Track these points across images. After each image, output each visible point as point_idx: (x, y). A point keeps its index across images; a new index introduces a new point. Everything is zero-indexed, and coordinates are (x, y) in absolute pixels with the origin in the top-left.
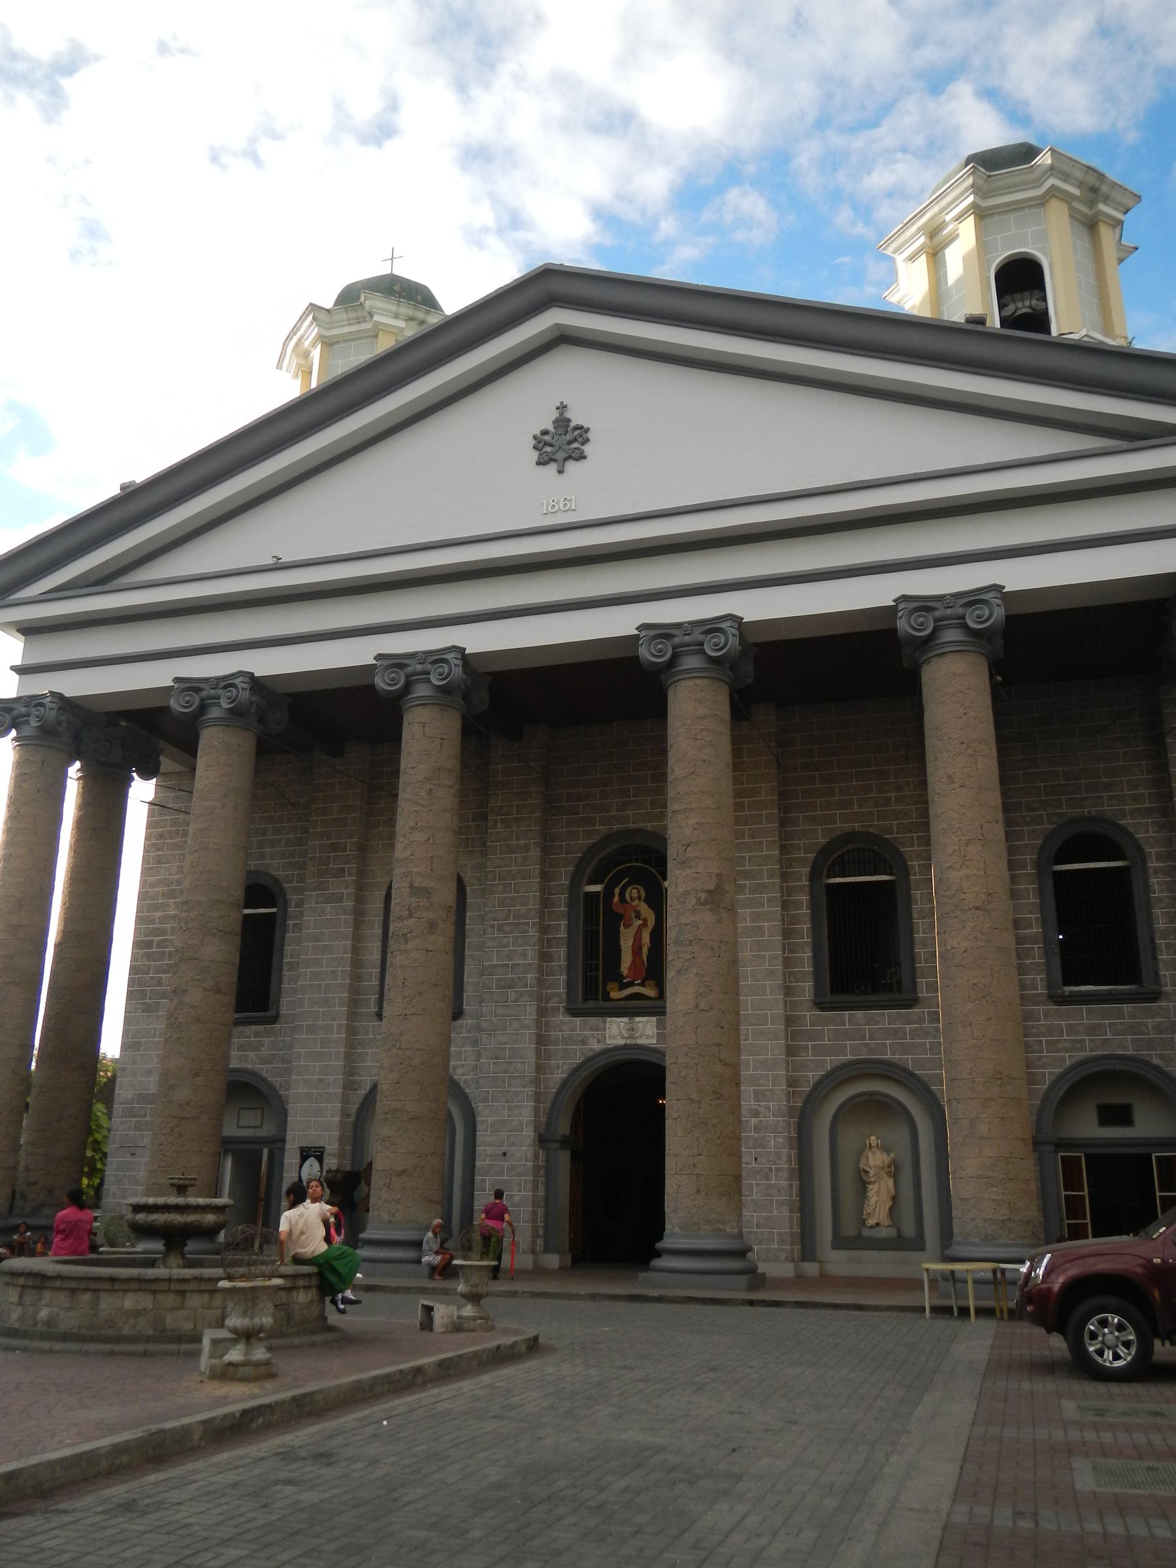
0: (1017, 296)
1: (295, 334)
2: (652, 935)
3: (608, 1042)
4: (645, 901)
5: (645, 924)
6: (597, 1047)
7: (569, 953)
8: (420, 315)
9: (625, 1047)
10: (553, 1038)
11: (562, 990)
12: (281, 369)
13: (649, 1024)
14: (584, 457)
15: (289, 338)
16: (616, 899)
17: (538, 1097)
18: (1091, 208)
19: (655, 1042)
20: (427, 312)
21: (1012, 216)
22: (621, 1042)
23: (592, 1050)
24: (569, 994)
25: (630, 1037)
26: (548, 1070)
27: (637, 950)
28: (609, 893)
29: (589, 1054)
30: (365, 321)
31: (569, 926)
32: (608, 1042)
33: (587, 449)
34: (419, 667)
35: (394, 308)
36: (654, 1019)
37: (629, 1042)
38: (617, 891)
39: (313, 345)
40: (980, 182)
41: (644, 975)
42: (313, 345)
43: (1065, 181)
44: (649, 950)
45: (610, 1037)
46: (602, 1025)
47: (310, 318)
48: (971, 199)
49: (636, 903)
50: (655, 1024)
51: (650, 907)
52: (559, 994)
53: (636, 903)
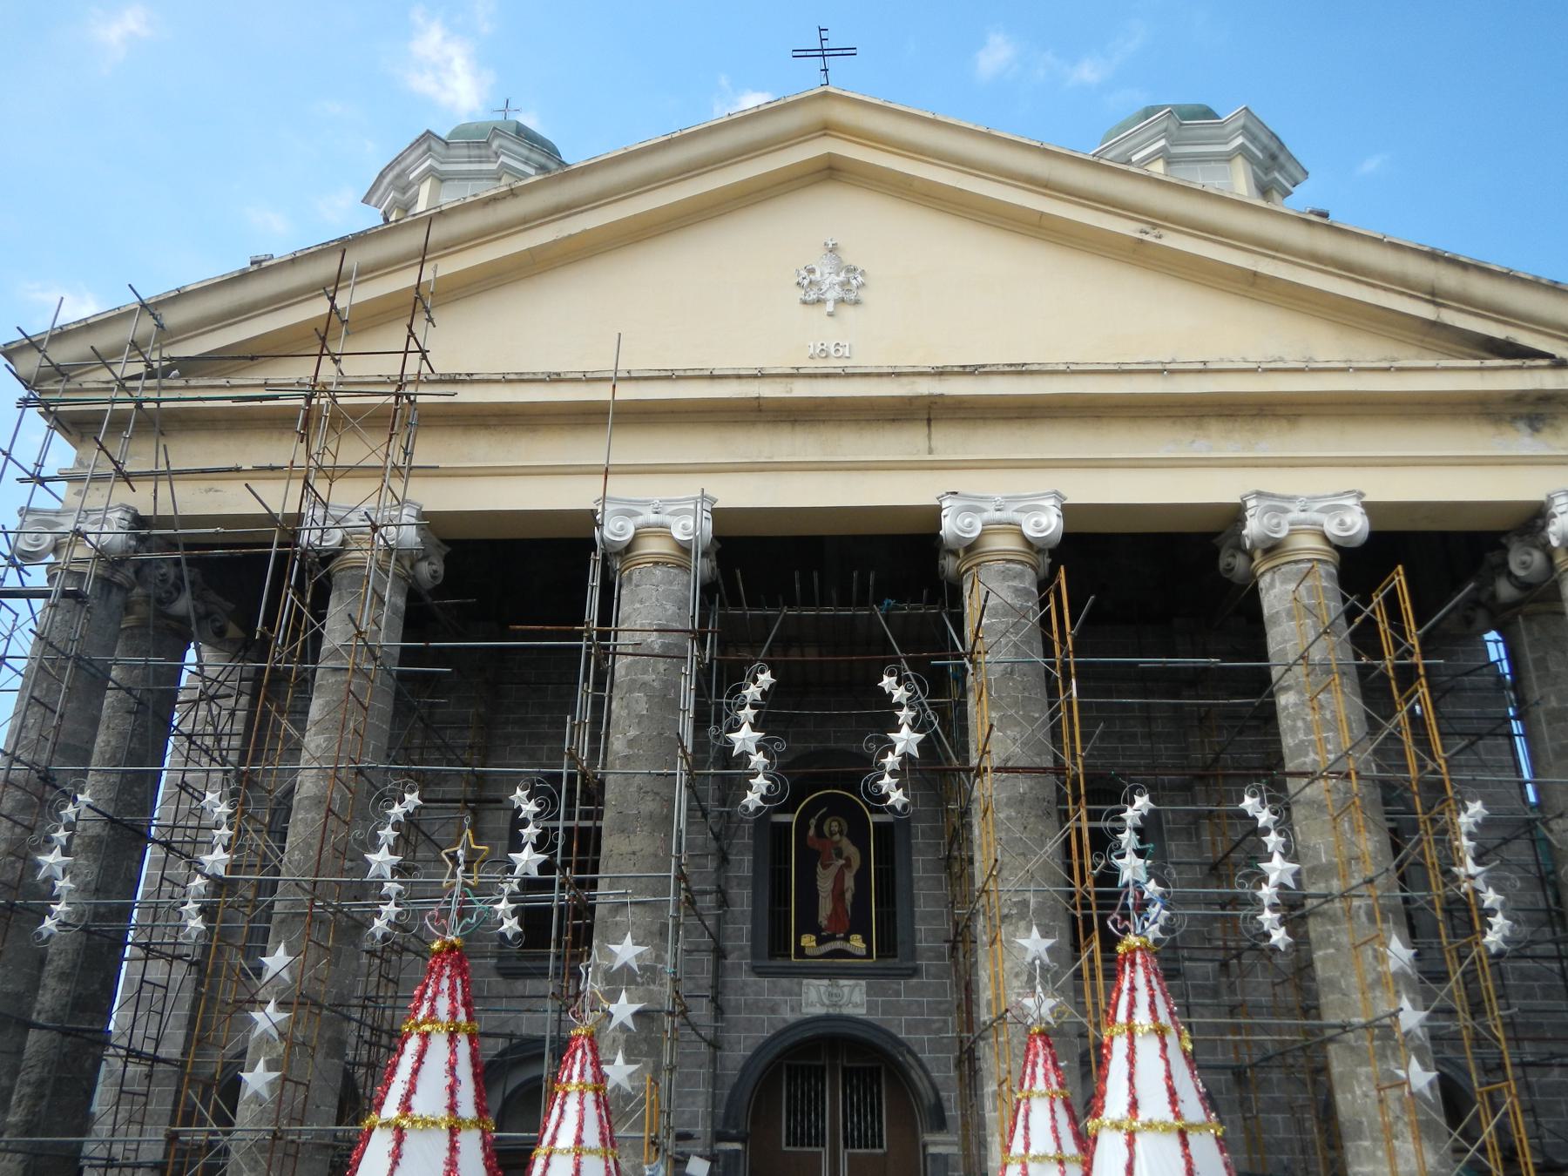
1: (399, 163)
2: (857, 878)
3: (804, 1010)
4: (848, 836)
5: (848, 865)
6: (790, 1017)
7: (754, 894)
9: (827, 1018)
10: (733, 1004)
11: (745, 942)
12: (368, 203)
13: (857, 989)
14: (857, 302)
15: (390, 167)
16: (812, 832)
17: (715, 1080)
18: (1266, 174)
19: (864, 1011)
21: (1199, 166)
22: (819, 1010)
23: (784, 1020)
24: (753, 947)
25: (835, 1005)
26: (726, 1046)
27: (838, 894)
28: (802, 824)
29: (781, 1026)
31: (755, 862)
32: (804, 1010)
33: (862, 294)
34: (653, 518)
35: (525, 152)
36: (863, 983)
37: (831, 1011)
38: (813, 822)
39: (422, 178)
40: (1173, 128)
41: (847, 924)
42: (422, 178)
43: (1251, 142)
44: (854, 896)
45: (807, 1005)
46: (796, 989)
47: (425, 146)
48: (1162, 143)
49: (837, 837)
50: (864, 989)
51: (854, 843)
52: (741, 948)
53: (837, 837)
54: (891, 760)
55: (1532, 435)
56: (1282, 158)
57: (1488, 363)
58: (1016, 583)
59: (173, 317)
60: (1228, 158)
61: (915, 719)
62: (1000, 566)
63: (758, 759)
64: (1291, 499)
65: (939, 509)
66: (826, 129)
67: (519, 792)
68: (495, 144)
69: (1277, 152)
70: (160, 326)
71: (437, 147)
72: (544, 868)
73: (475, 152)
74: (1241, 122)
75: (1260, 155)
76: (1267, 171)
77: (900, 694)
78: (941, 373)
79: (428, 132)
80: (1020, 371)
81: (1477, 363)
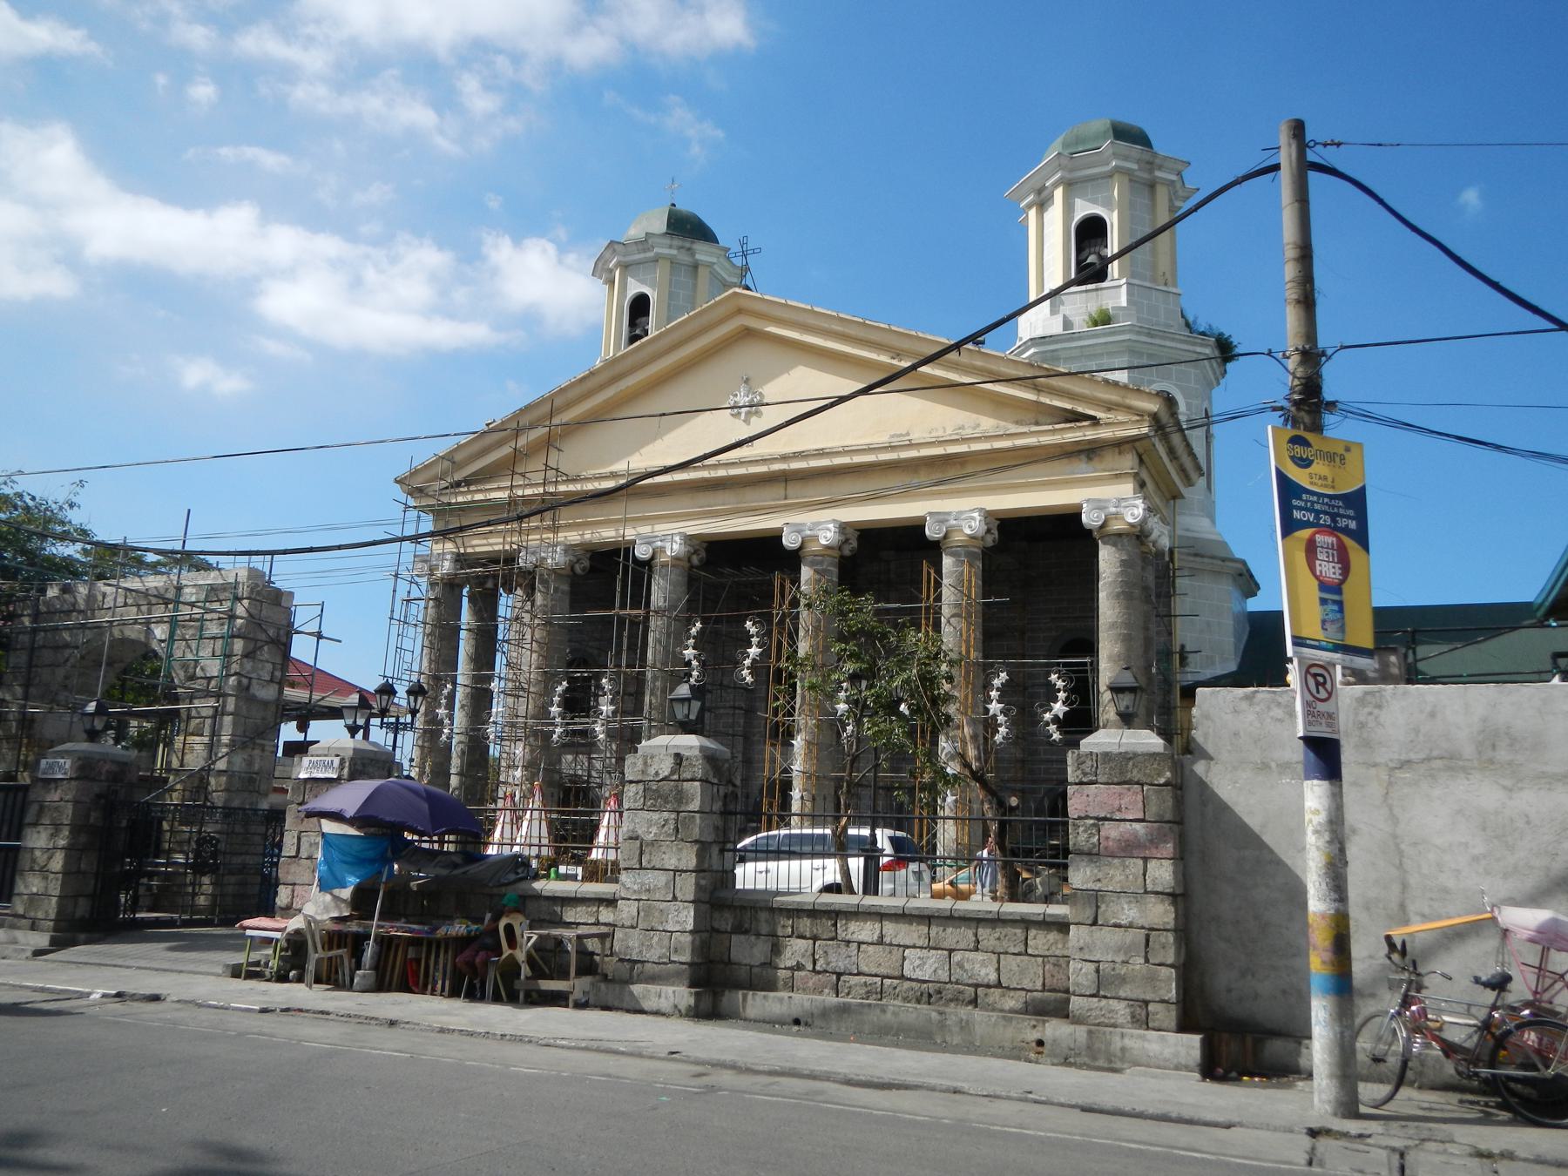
0: (1093, 241)
8: (687, 245)
20: (692, 242)
30: (649, 250)
40: (1064, 161)
42: (616, 266)
54: (747, 662)
55: (1087, 463)
56: (1157, 161)
57: (1057, 426)
58: (819, 567)
59: (458, 457)
60: (1110, 175)
61: (759, 642)
62: (810, 558)
63: (695, 663)
64: (949, 513)
65: (781, 530)
66: (740, 311)
67: (604, 680)
68: (650, 241)
69: (1151, 160)
70: (454, 463)
71: (616, 246)
72: (614, 713)
73: (640, 247)
74: (1111, 151)
75: (1135, 167)
76: (1151, 171)
77: (753, 630)
78: (784, 458)
79: (612, 242)
80: (821, 453)
81: (1050, 427)
